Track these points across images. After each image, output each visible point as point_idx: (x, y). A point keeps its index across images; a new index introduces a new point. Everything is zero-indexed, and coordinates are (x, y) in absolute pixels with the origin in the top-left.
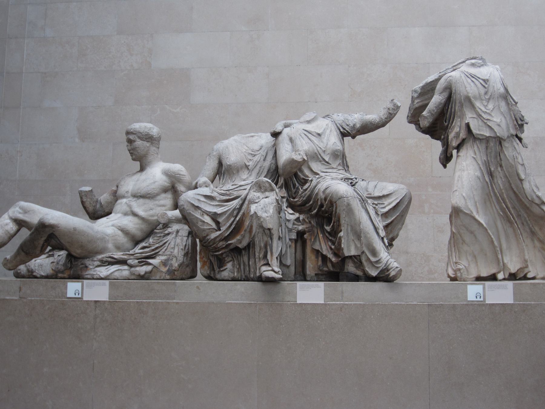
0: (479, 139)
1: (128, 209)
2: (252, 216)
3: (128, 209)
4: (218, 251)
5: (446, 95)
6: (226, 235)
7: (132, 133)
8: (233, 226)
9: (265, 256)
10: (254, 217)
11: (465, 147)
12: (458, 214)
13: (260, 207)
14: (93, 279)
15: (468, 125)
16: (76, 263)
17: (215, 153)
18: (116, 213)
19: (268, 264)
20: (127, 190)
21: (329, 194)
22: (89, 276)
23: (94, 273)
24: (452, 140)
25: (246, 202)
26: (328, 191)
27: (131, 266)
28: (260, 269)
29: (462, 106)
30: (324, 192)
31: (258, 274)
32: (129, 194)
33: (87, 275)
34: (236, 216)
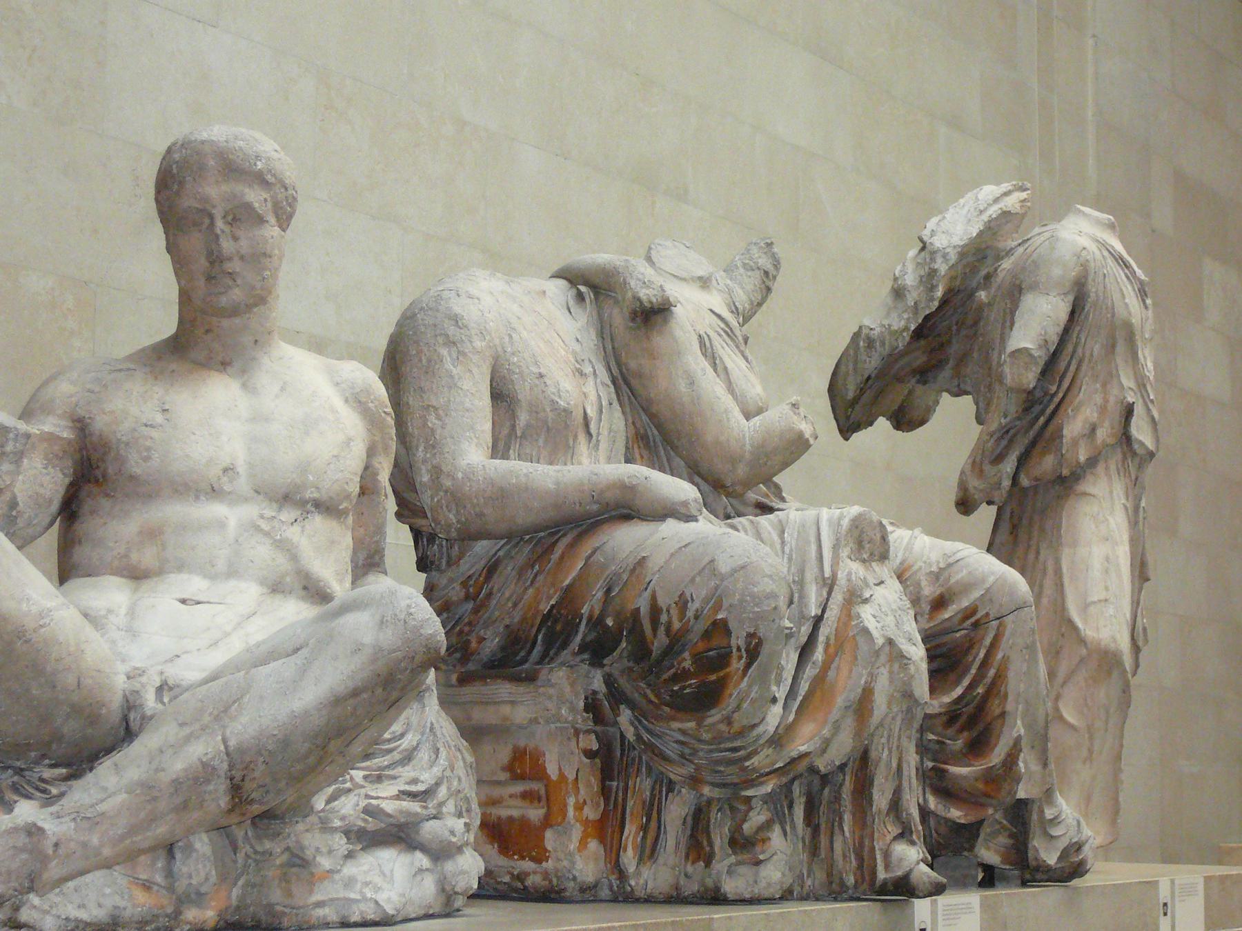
0: (1134, 454)
1: (282, 562)
2: (877, 653)
3: (282, 562)
4: (750, 783)
5: (1071, 298)
6: (791, 718)
7: (260, 179)
8: (804, 687)
9: (895, 805)
10: (883, 658)
11: (1100, 468)
12: (1109, 673)
13: (890, 620)
14: (345, 924)
15: (1129, 411)
16: (268, 845)
17: (478, 344)
18: (213, 577)
19: (905, 834)
20: (226, 461)
21: (966, 587)
22: (328, 913)
23: (352, 896)
24: (1075, 443)
25: (838, 597)
26: (959, 576)
27: (440, 853)
28: (887, 855)
29: (1111, 348)
30: (936, 576)
31: (882, 875)
32: (243, 484)
33: (320, 904)
34: (805, 651)
